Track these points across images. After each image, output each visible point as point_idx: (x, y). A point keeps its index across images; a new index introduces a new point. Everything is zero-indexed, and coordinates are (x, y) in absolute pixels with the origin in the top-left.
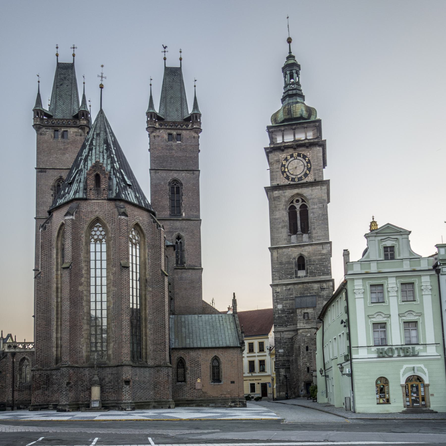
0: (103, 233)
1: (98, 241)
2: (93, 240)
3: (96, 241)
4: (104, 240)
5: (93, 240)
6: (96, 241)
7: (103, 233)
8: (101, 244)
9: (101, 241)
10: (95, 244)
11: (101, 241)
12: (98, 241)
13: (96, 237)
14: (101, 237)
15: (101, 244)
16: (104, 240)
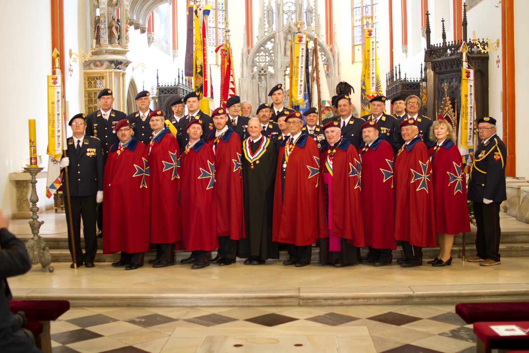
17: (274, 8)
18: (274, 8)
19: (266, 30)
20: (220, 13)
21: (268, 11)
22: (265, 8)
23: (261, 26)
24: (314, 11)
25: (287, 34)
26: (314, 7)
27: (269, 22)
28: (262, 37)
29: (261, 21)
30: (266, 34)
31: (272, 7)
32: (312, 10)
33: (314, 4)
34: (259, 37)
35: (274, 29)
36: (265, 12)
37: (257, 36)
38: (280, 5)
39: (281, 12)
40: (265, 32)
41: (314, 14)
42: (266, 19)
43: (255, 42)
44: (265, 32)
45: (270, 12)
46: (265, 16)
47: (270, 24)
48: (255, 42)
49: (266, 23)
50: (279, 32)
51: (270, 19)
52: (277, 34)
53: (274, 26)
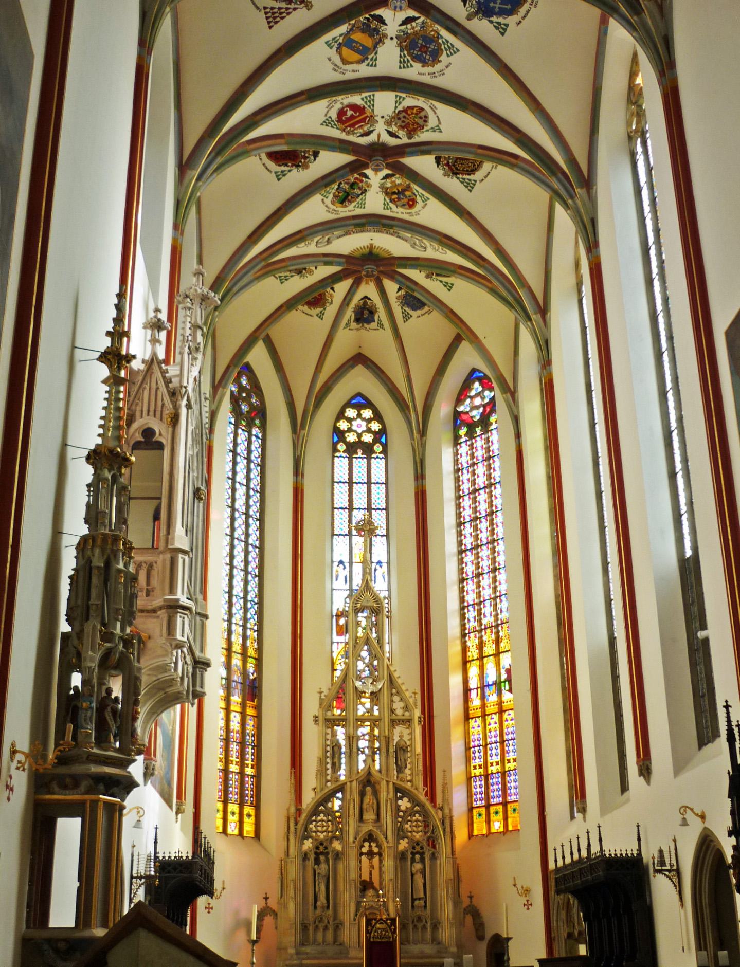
0: (375, 426)
1: (360, 452)
2: (341, 447)
3: (351, 449)
4: (378, 448)
5: (341, 447)
6: (351, 449)
7: (375, 426)
8: (369, 459)
9: (368, 449)
10: (350, 459)
11: (368, 449)
12: (360, 452)
13: (351, 438)
14: (368, 438)
15: (369, 459)
16: (378, 448)
17: (343, 743)
18: (343, 743)
19: (329, 778)
20: (249, 750)
21: (333, 747)
22: (328, 743)
23: (322, 772)
24: (409, 749)
25: (364, 787)
26: (408, 743)
27: (334, 765)
28: (322, 790)
29: (322, 762)
30: (329, 784)
31: (338, 741)
32: (407, 748)
33: (409, 737)
34: (318, 790)
35: (343, 778)
36: (328, 748)
37: (314, 787)
38: (353, 737)
39: (355, 750)
40: (327, 781)
41: (409, 754)
42: (328, 760)
43: (309, 798)
44: (327, 781)
45: (336, 749)
46: (328, 754)
47: (336, 767)
48: (309, 798)
49: (329, 766)
50: (351, 782)
51: (336, 760)
52: (348, 784)
53: (342, 772)
